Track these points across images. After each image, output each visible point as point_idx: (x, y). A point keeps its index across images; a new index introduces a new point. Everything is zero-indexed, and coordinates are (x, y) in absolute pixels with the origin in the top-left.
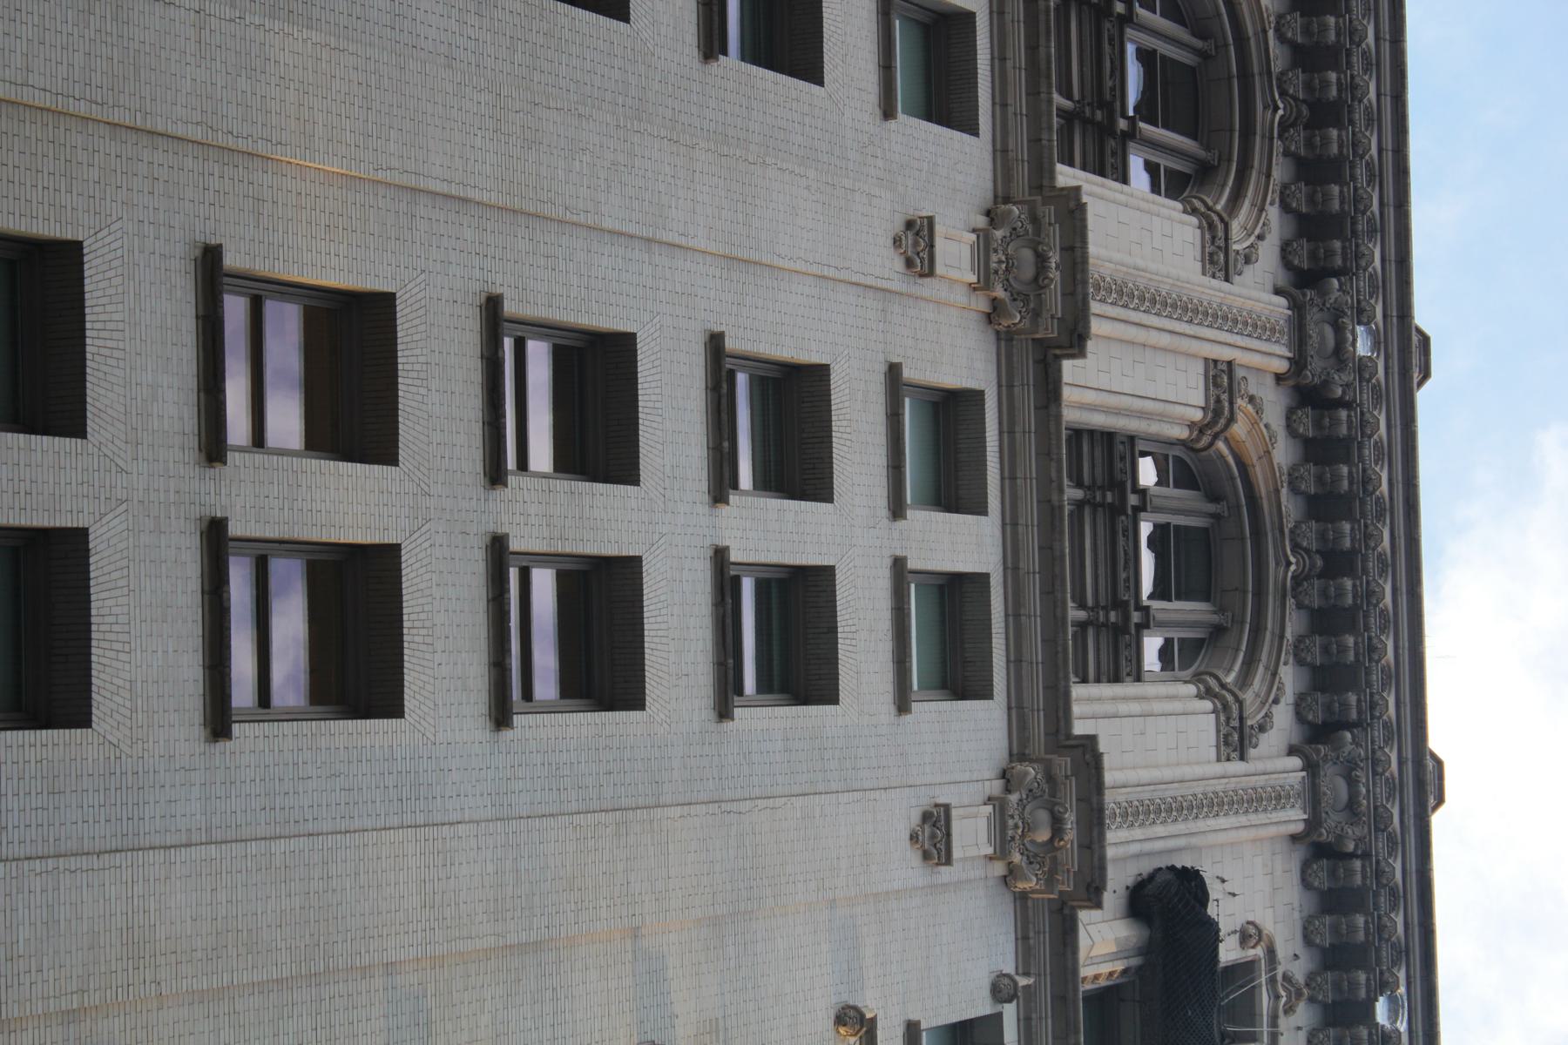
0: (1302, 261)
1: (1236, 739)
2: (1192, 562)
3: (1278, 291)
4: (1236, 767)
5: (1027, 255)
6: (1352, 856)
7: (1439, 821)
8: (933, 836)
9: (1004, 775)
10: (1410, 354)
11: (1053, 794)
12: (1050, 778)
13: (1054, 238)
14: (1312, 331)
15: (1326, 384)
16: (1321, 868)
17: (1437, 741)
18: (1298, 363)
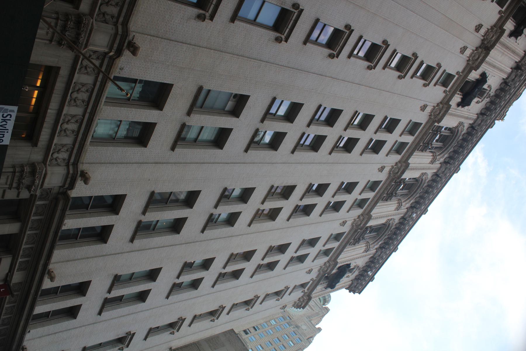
0: (483, 112)
1: (432, 162)
2: (444, 139)
3: (511, 68)
4: (431, 165)
5: (439, 111)
9: (438, 104)
10: (372, 279)
12: (443, 107)
13: (444, 109)
14: (512, 75)
16: (470, 129)
17: (429, 209)
18: (507, 78)
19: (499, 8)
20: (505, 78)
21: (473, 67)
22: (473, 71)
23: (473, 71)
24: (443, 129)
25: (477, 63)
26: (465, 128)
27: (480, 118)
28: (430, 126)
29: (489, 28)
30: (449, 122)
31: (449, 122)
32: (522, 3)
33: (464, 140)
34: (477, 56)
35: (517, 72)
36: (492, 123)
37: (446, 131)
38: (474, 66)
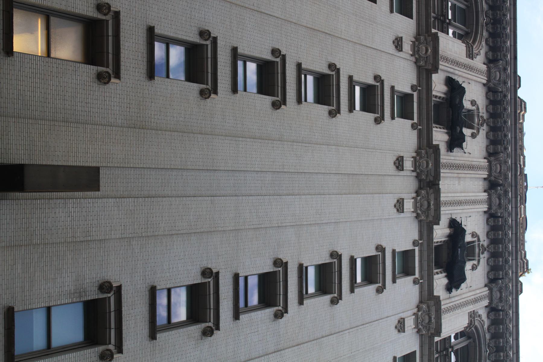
3: (485, 191)
5: (427, 317)
6: (501, 310)
7: (521, 297)
8: (401, 326)
9: (418, 307)
11: (429, 311)
12: (428, 307)
13: (433, 309)
15: (497, 306)
18: (490, 208)
19: (409, 122)
20: (486, 209)
21: (430, 222)
22: (435, 227)
23: (435, 227)
24: (453, 340)
25: (432, 212)
26: (484, 317)
27: (495, 289)
28: (430, 349)
29: (414, 154)
30: (453, 324)
31: (453, 324)
32: (434, 99)
33: (495, 336)
34: (426, 203)
35: (496, 191)
36: (517, 286)
37: (460, 340)
38: (431, 219)
